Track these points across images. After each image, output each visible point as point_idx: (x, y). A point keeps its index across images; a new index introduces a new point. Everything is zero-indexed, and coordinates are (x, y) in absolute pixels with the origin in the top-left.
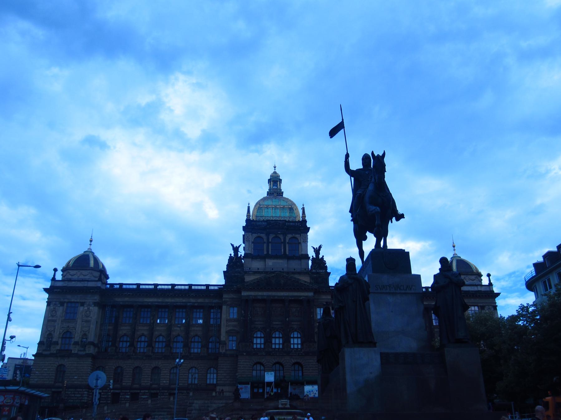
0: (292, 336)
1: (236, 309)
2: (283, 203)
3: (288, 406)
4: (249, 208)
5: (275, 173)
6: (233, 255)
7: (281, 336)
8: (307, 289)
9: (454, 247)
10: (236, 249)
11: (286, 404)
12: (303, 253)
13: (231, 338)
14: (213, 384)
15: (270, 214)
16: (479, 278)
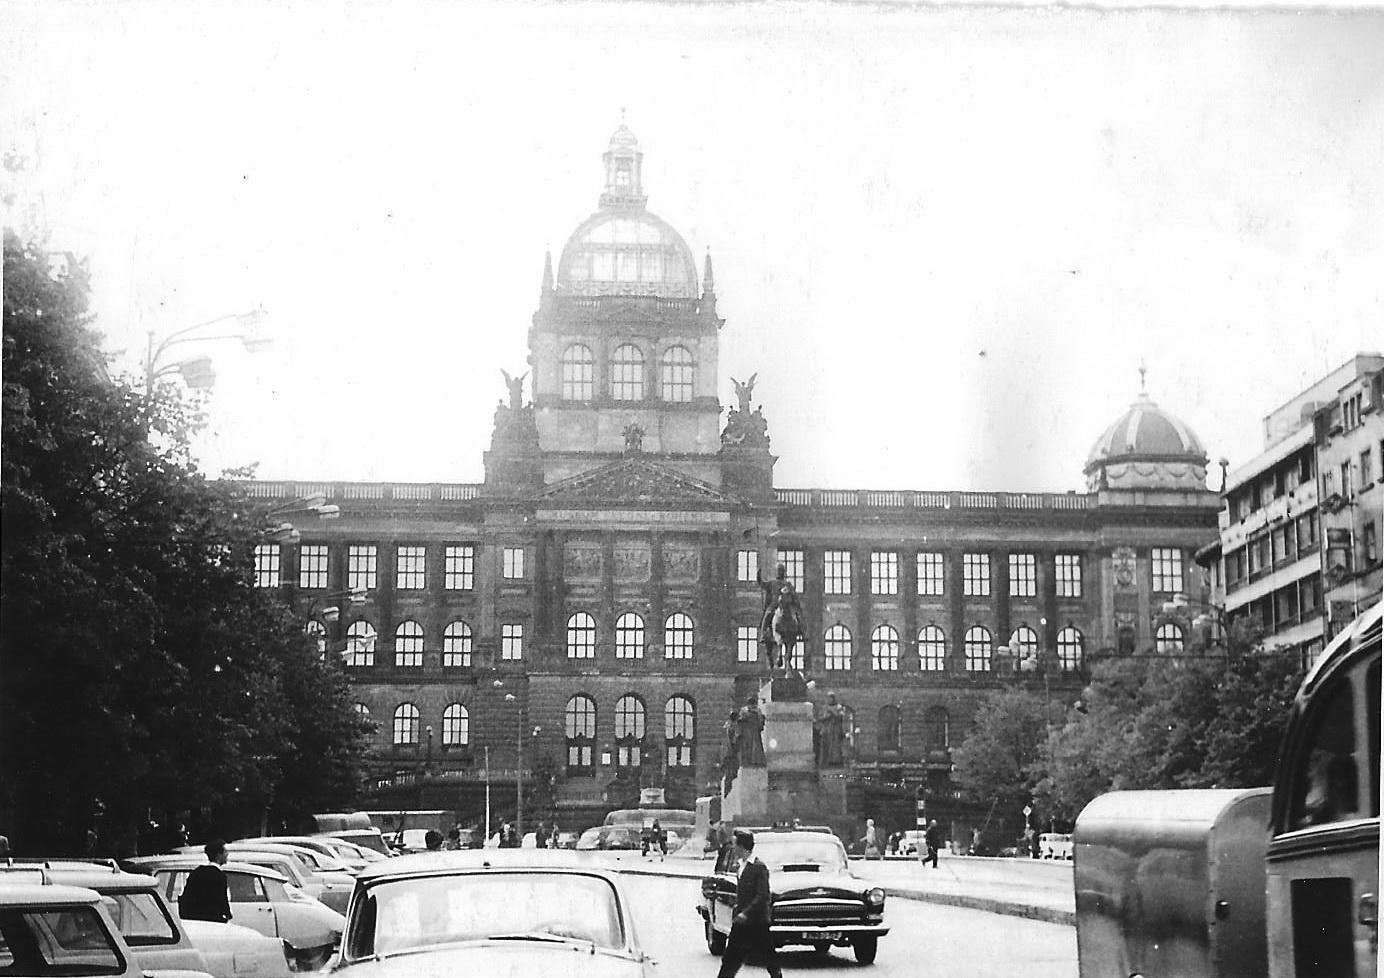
0: (669, 625)
1: (519, 553)
2: (649, 235)
3: (662, 800)
4: (549, 259)
5: (623, 128)
6: (507, 403)
7: (640, 624)
8: (713, 508)
9: (1142, 372)
10: (515, 386)
11: (655, 797)
12: (707, 392)
13: (507, 630)
14: (459, 745)
15: (609, 273)
16: (1199, 470)
